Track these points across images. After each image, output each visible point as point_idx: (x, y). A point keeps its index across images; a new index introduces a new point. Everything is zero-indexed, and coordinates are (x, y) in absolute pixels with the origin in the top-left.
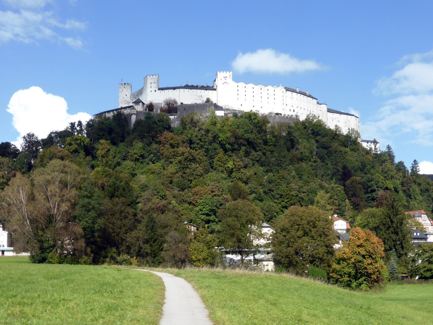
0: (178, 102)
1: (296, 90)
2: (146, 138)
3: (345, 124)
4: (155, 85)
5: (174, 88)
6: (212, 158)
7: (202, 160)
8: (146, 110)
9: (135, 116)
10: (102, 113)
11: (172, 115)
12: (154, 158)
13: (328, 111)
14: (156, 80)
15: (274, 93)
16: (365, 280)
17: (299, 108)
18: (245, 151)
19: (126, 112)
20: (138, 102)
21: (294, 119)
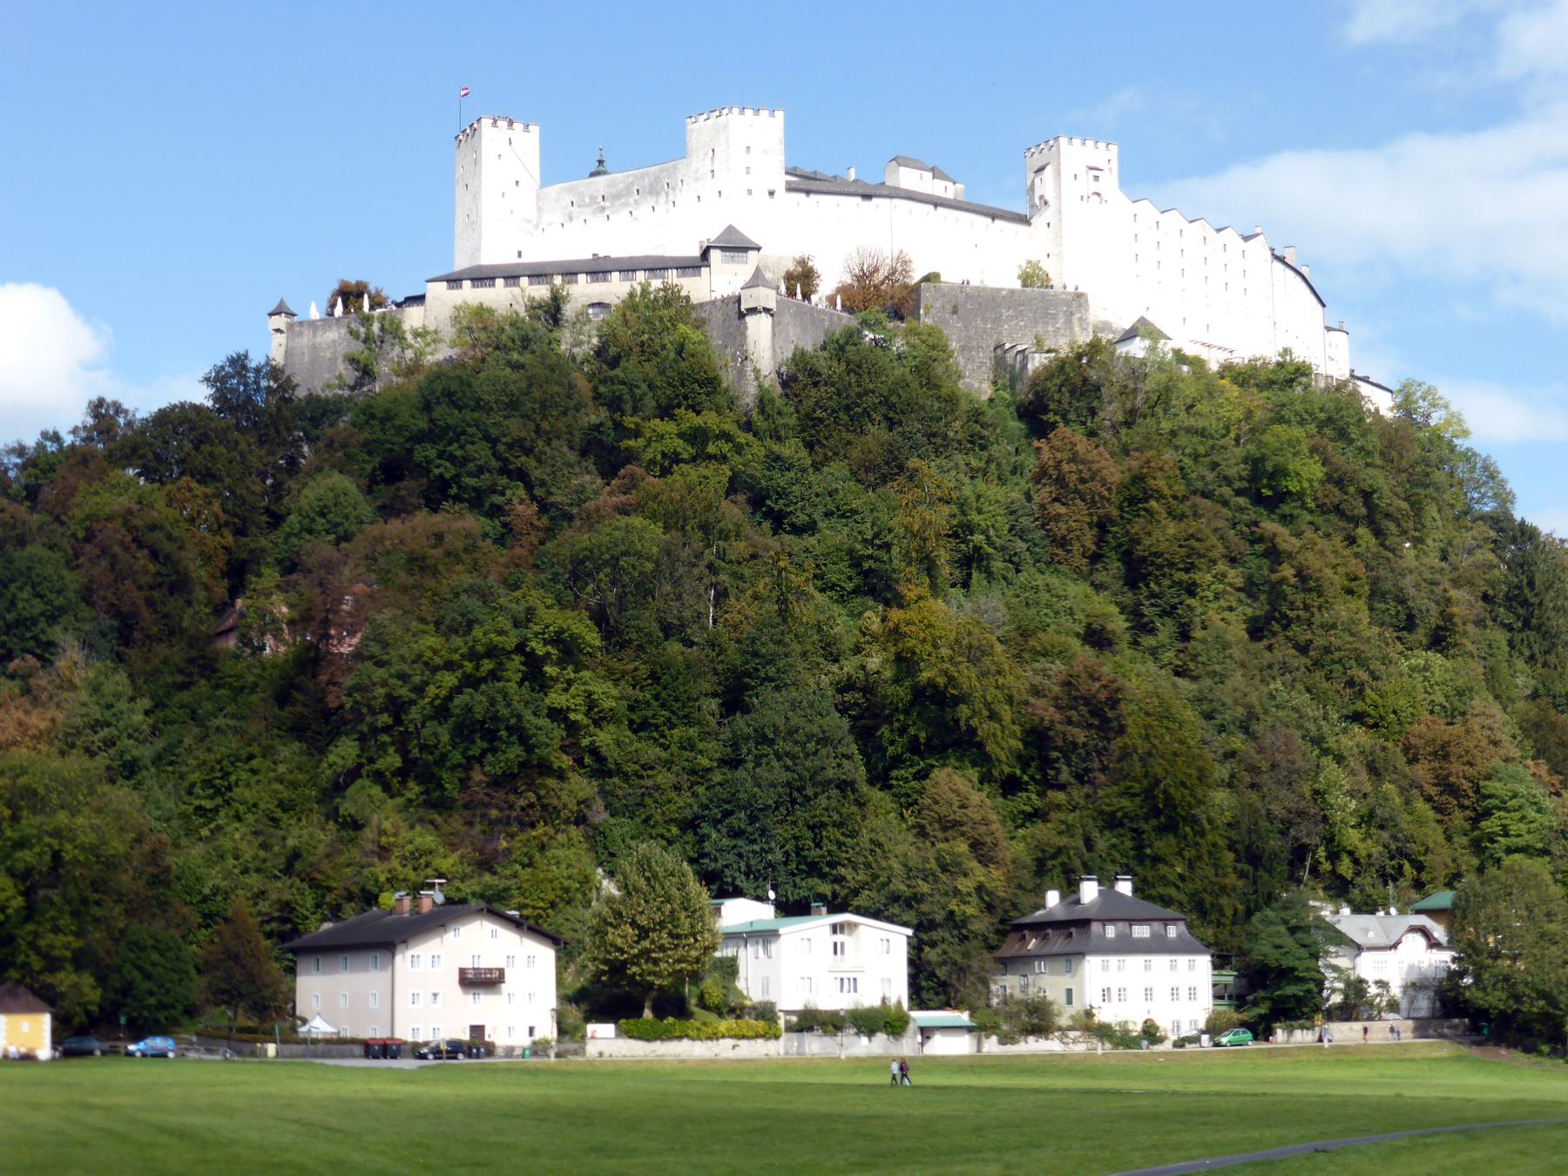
9: (770, 318)
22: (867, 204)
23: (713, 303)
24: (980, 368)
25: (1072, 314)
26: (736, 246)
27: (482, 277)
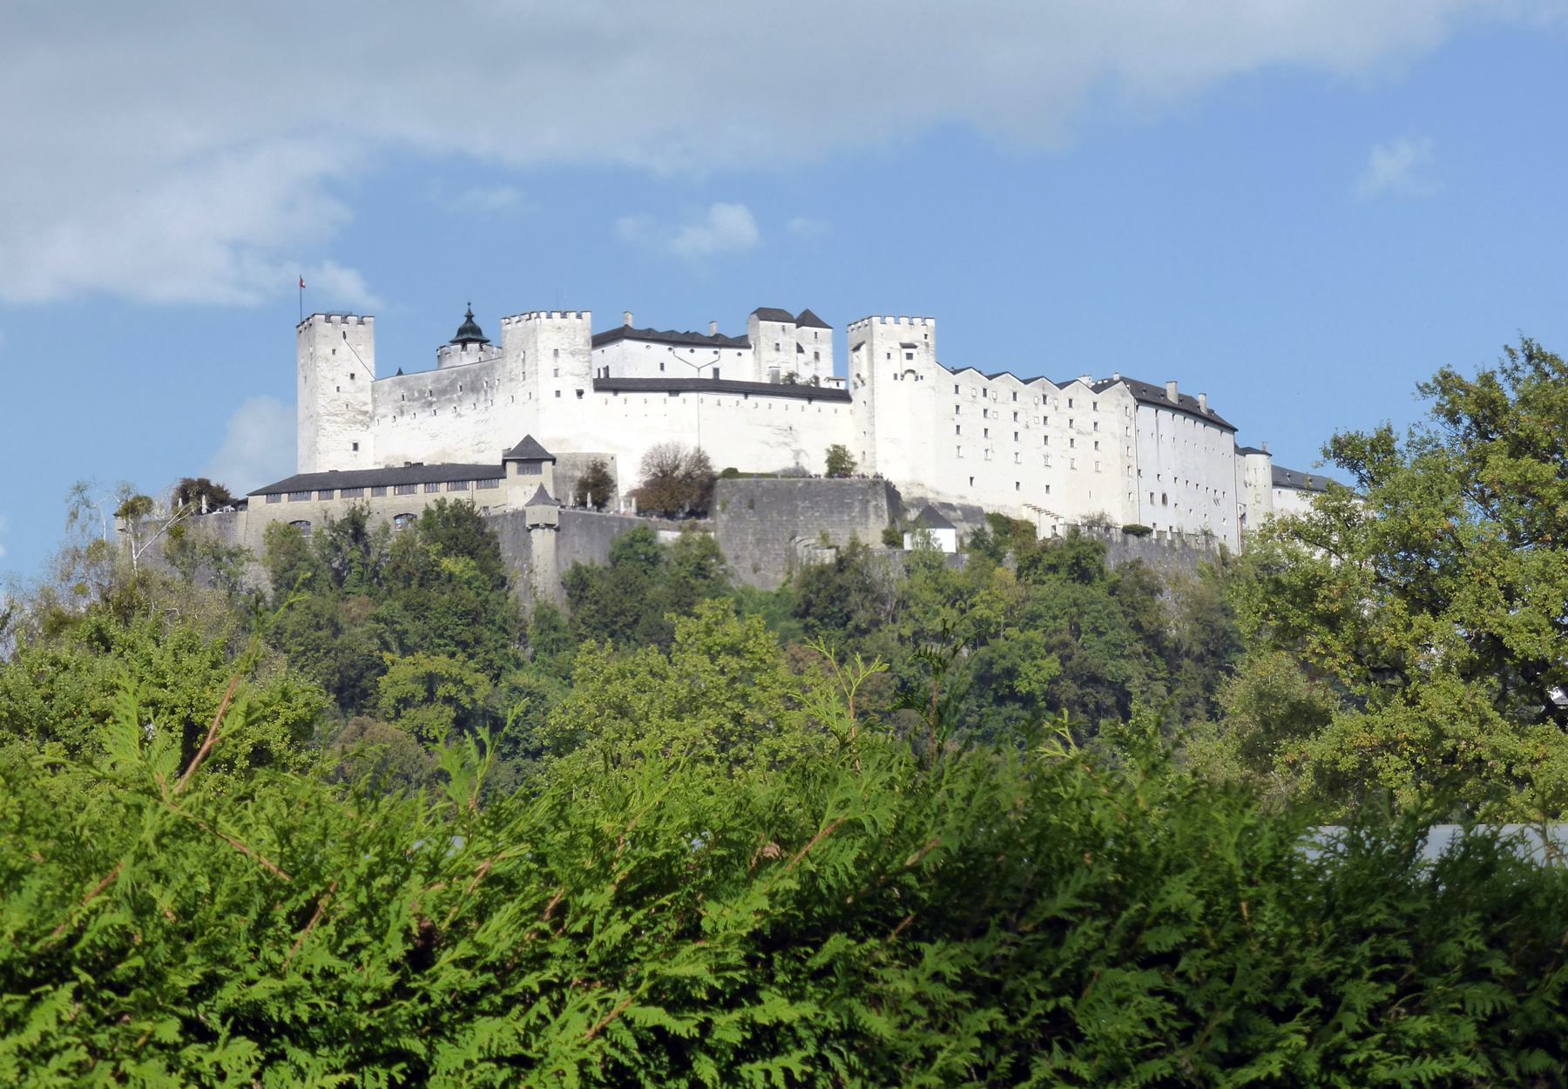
1: (1163, 393)
9: (550, 535)
13: (1276, 484)
22: (674, 399)
23: (505, 515)
24: (775, 559)
25: (868, 502)
26: (529, 456)
27: (300, 486)
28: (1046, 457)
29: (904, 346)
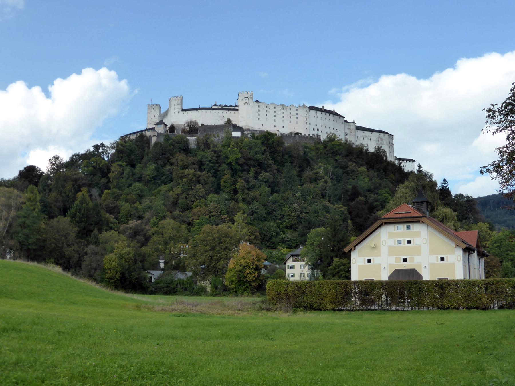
0: (199, 123)
2: (161, 160)
3: (377, 142)
4: (179, 107)
5: (197, 109)
6: (220, 179)
7: (207, 182)
8: (167, 132)
10: (126, 136)
11: (193, 136)
12: (166, 180)
14: (179, 102)
15: (297, 112)
16: (247, 287)
17: (324, 127)
18: (255, 172)
19: (148, 134)
20: (161, 123)
21: (315, 138)
28: (283, 120)
29: (245, 98)
